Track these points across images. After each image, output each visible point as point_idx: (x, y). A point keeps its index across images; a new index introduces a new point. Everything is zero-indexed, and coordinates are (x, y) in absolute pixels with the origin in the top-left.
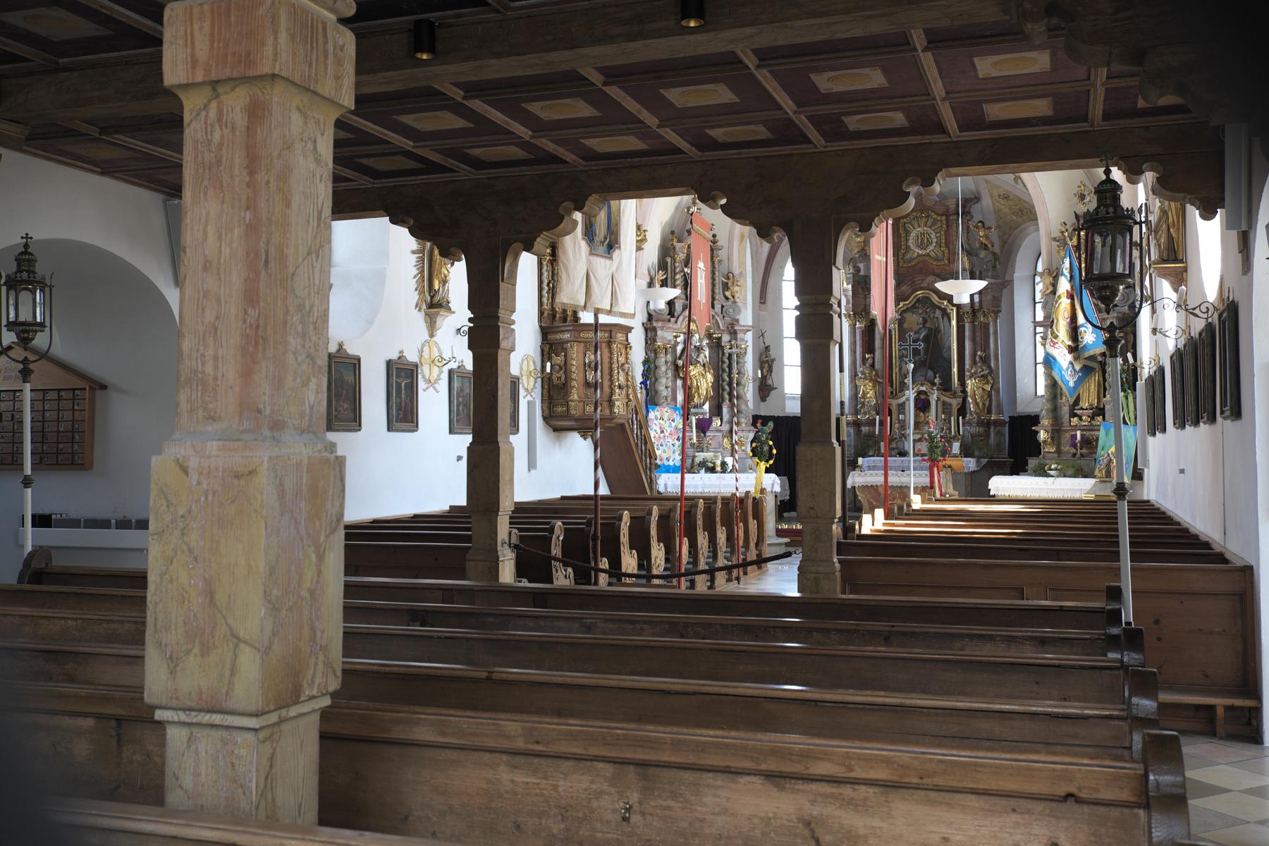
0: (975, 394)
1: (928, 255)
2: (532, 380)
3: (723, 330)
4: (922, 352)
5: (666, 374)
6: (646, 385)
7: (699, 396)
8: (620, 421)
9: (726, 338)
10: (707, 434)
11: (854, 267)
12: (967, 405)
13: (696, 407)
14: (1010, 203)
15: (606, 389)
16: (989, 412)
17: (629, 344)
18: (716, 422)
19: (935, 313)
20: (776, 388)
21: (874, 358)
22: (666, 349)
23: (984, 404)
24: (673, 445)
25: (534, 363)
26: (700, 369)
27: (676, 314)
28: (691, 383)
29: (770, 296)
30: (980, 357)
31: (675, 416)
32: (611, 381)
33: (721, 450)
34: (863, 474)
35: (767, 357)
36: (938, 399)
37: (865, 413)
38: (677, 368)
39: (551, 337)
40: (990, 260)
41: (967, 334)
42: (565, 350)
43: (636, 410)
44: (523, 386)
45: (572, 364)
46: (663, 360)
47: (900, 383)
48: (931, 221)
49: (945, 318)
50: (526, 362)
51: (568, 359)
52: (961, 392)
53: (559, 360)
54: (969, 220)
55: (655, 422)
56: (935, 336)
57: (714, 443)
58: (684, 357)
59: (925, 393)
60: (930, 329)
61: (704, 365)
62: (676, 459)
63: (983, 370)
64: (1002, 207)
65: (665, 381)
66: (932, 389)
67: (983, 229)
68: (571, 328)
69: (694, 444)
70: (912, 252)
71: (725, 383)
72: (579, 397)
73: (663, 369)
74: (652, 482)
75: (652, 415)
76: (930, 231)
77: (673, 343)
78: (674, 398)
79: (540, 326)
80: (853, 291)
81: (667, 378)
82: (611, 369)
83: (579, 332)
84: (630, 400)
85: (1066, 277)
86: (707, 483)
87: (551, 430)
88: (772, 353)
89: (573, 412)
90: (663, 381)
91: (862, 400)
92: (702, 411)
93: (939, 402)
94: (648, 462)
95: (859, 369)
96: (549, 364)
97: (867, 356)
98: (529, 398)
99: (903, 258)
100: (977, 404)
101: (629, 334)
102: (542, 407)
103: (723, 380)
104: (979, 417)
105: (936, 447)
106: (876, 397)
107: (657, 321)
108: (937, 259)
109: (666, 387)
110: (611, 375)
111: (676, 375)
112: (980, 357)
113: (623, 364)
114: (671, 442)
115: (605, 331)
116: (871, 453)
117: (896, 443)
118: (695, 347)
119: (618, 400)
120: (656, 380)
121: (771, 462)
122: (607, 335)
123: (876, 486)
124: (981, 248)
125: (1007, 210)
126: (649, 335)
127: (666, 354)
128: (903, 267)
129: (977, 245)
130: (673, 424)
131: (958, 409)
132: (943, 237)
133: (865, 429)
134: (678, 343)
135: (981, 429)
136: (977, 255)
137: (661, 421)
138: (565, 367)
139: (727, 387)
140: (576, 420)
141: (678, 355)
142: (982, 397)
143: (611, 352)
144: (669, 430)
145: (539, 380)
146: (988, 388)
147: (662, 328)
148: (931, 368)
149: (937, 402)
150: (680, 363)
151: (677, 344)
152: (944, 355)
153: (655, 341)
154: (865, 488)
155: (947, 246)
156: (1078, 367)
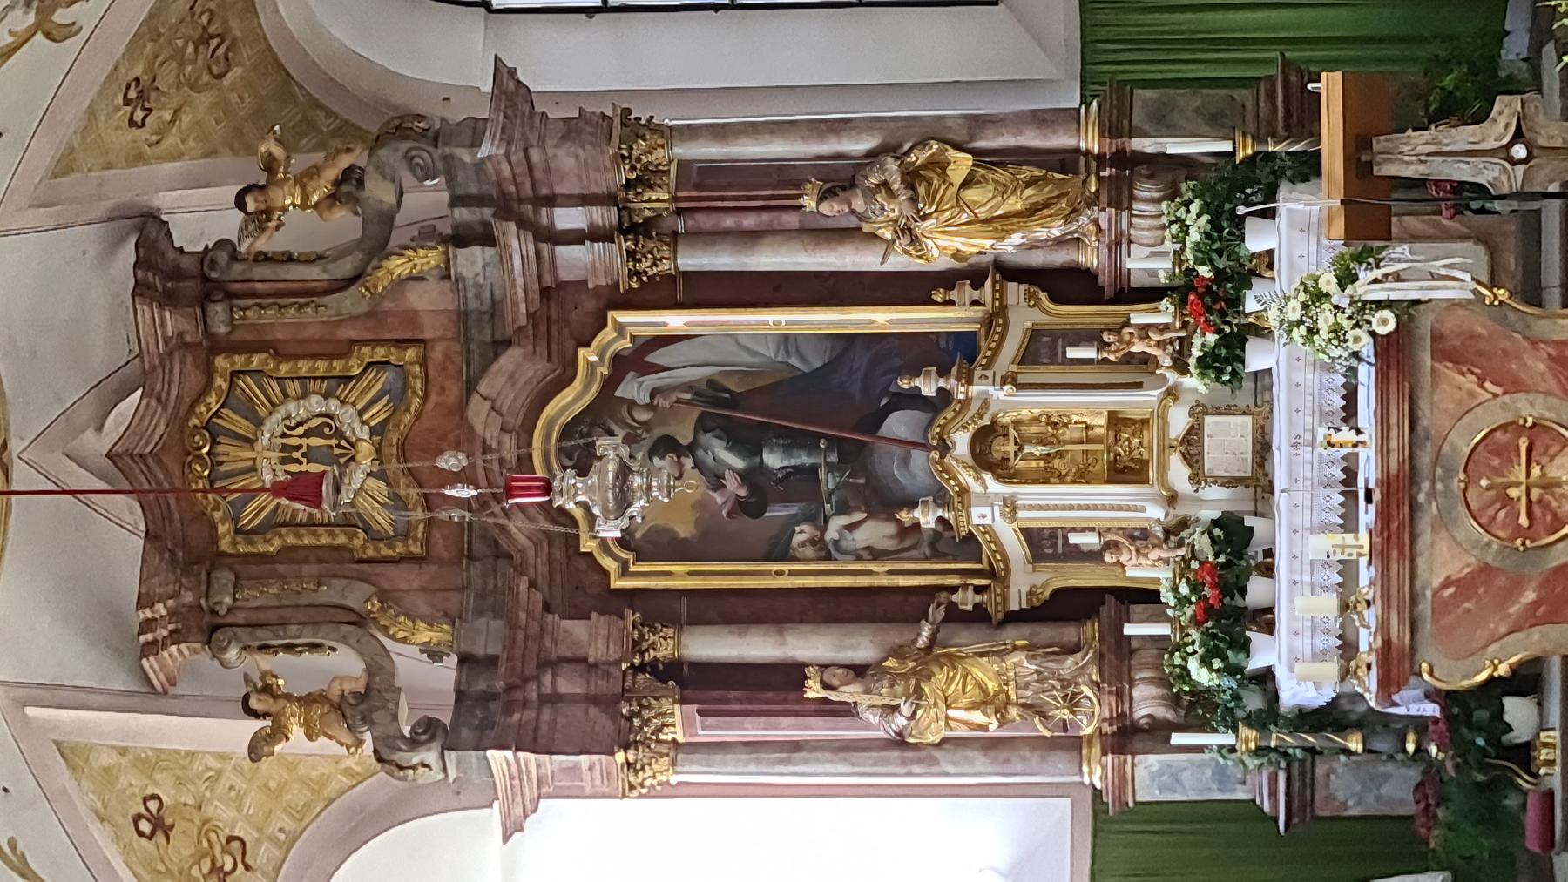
1: (378, 431)
4: (803, 459)
11: (414, 743)
12: (1037, 259)
14: (166, 80)
16: (1066, 161)
19: (632, 404)
21: (824, 667)
23: (1031, 183)
36: (1009, 379)
37: (1072, 702)
40: (409, 158)
47: (937, 555)
48: (235, 422)
49: (658, 357)
52: (977, 284)
54: (234, 256)
56: (734, 401)
60: (703, 425)
64: (186, 119)
66: (966, 403)
70: (364, 504)
76: (274, 423)
93: (1022, 379)
95: (875, 727)
99: (388, 540)
100: (1032, 211)
104: (1092, 201)
106: (1000, 654)
108: (398, 396)
112: (821, 199)
124: (353, 201)
131: (1055, 300)
132: (304, 367)
135: (1143, 190)
142: (1003, 190)
146: (960, 165)
152: (817, 364)
155: (344, 350)
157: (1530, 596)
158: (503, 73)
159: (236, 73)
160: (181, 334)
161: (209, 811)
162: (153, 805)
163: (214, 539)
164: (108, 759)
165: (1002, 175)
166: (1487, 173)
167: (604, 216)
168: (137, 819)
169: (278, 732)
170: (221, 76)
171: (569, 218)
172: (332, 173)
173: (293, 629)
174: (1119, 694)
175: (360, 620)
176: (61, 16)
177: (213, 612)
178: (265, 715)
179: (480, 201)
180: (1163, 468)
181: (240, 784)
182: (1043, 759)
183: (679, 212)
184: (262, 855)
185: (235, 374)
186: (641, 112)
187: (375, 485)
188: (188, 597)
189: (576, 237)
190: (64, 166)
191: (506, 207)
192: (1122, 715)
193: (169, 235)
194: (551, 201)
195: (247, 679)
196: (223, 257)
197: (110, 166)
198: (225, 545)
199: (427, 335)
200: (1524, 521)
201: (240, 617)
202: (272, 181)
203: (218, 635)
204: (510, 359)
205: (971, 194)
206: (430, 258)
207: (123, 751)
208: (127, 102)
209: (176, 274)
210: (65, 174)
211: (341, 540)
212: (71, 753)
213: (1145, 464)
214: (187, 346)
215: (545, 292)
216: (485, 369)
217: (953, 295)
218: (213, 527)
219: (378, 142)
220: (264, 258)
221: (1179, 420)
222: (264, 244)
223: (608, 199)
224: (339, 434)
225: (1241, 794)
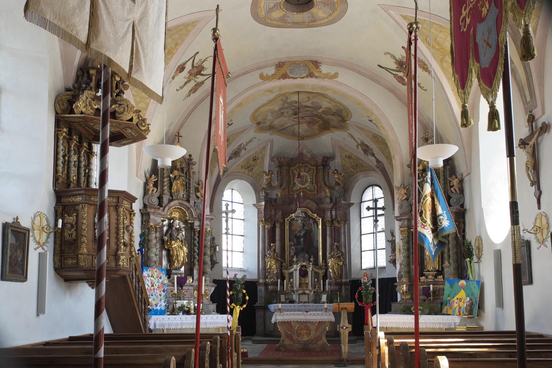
0: (333, 267)
1: (306, 188)
2: (44, 235)
3: (195, 218)
5: (156, 246)
6: (142, 252)
7: (178, 262)
8: (124, 273)
9: (197, 223)
10: (184, 288)
11: (265, 192)
12: (328, 274)
13: (176, 269)
14: (352, 160)
15: (113, 246)
16: (341, 277)
17: (133, 211)
18: (190, 280)
20: (218, 263)
21: (275, 246)
22: (156, 228)
23: (338, 273)
24: (160, 295)
25: (47, 220)
26: (179, 243)
27: (164, 205)
28: (173, 253)
29: (215, 207)
30: (336, 246)
31: (162, 275)
32: (118, 239)
33: (193, 298)
34: (282, 314)
35: (213, 244)
36: (313, 270)
37: (271, 278)
38: (163, 242)
39: (65, 200)
41: (328, 233)
42: (77, 211)
43: (136, 268)
44: (35, 238)
45: (83, 223)
46: (154, 235)
47: (290, 261)
49: (315, 224)
50: (38, 218)
51: (79, 220)
52: (325, 266)
53: (71, 219)
54: (328, 169)
55: (148, 278)
57: (188, 294)
58: (168, 235)
59: (305, 266)
60: (307, 230)
61: (182, 241)
62: (162, 305)
63: (338, 254)
64: (346, 163)
65: (155, 251)
67: (337, 174)
68: (83, 192)
69: (175, 294)
71: (195, 254)
72: (88, 252)
73: (154, 241)
74: (145, 322)
75: (145, 274)
76: (307, 174)
77: (161, 224)
78: (161, 263)
79: (55, 190)
80: (265, 206)
81: (157, 249)
82: (118, 229)
83: (91, 196)
84: (133, 256)
85: (429, 183)
86: (184, 321)
87: (63, 280)
88: (216, 241)
89: (82, 264)
90: (154, 250)
91: (269, 270)
92: (180, 272)
93: (313, 272)
94: (143, 307)
96: (60, 221)
97: (272, 245)
98: (40, 250)
99: (291, 189)
101: (133, 204)
102: (54, 259)
103: (194, 252)
104: (336, 280)
105: (370, 294)
106: (277, 269)
107: (151, 208)
108: (310, 191)
109: (156, 255)
110: (117, 233)
111: (162, 247)
112: (336, 245)
113: (128, 226)
114: (159, 293)
115: (113, 197)
116: (275, 302)
117: (288, 296)
118: (176, 228)
119: (123, 255)
120: (149, 249)
121: (245, 306)
122: (114, 200)
123: (290, 322)
125: (349, 165)
126: (144, 218)
127: (156, 232)
128: (291, 194)
129: (334, 183)
130: (160, 281)
131: (323, 276)
132: (314, 178)
133: (270, 287)
134: (164, 225)
135: (337, 287)
136: (333, 189)
137: (152, 278)
138: (77, 225)
139: (197, 257)
140: (85, 271)
141: (164, 233)
142: (337, 269)
143: (118, 215)
144: (157, 285)
145: (52, 235)
146: (341, 263)
147: (154, 213)
148: (308, 253)
149: (312, 271)
150: (166, 238)
151: (163, 226)
152: (315, 245)
153: (148, 222)
154: (283, 323)
155: (317, 184)
156: (435, 243)
157: (289, 333)
158: (352, 204)
159: (353, 170)
160: (318, 162)
161: (256, 166)
162: (257, 159)
163: (292, 167)
164: (263, 153)
165: (339, 269)
166: (342, 324)
167: (334, 216)
168: (256, 157)
169: (267, 175)
170: (352, 168)
171: (334, 213)
172: (339, 182)
173: (280, 177)
174: (271, 284)
175: (281, 186)
176: (360, 147)
177: (282, 167)
178: (269, 173)
179: (336, 201)
180: (301, 290)
181: (260, 170)
182: (263, 274)
183: (334, 227)
184: (250, 173)
185: (313, 169)
186: (347, 222)
187: (299, 188)
188: (284, 163)
189: (331, 214)
190: (340, 147)
191: (335, 204)
192: (269, 284)
193: (331, 161)
194: (336, 210)
195: (273, 171)
196: (328, 168)
197: (340, 153)
198: (291, 168)
199: (318, 194)
200: (299, 332)
201: (282, 170)
202: (338, 174)
203: (279, 167)
204: (315, 205)
205: (337, 265)
206: (328, 194)
207: (264, 155)
208: (349, 155)
209: (326, 162)
210: (339, 148)
211: (292, 183)
212: (264, 148)
213: (302, 288)
214: (317, 163)
215: (324, 209)
216: (314, 202)
217: (324, 263)
218: (294, 166)
219: (344, 188)
220: (328, 173)
221: (307, 292)
222: (330, 173)
223: (336, 218)
224: (305, 183)
225: (258, 300)
